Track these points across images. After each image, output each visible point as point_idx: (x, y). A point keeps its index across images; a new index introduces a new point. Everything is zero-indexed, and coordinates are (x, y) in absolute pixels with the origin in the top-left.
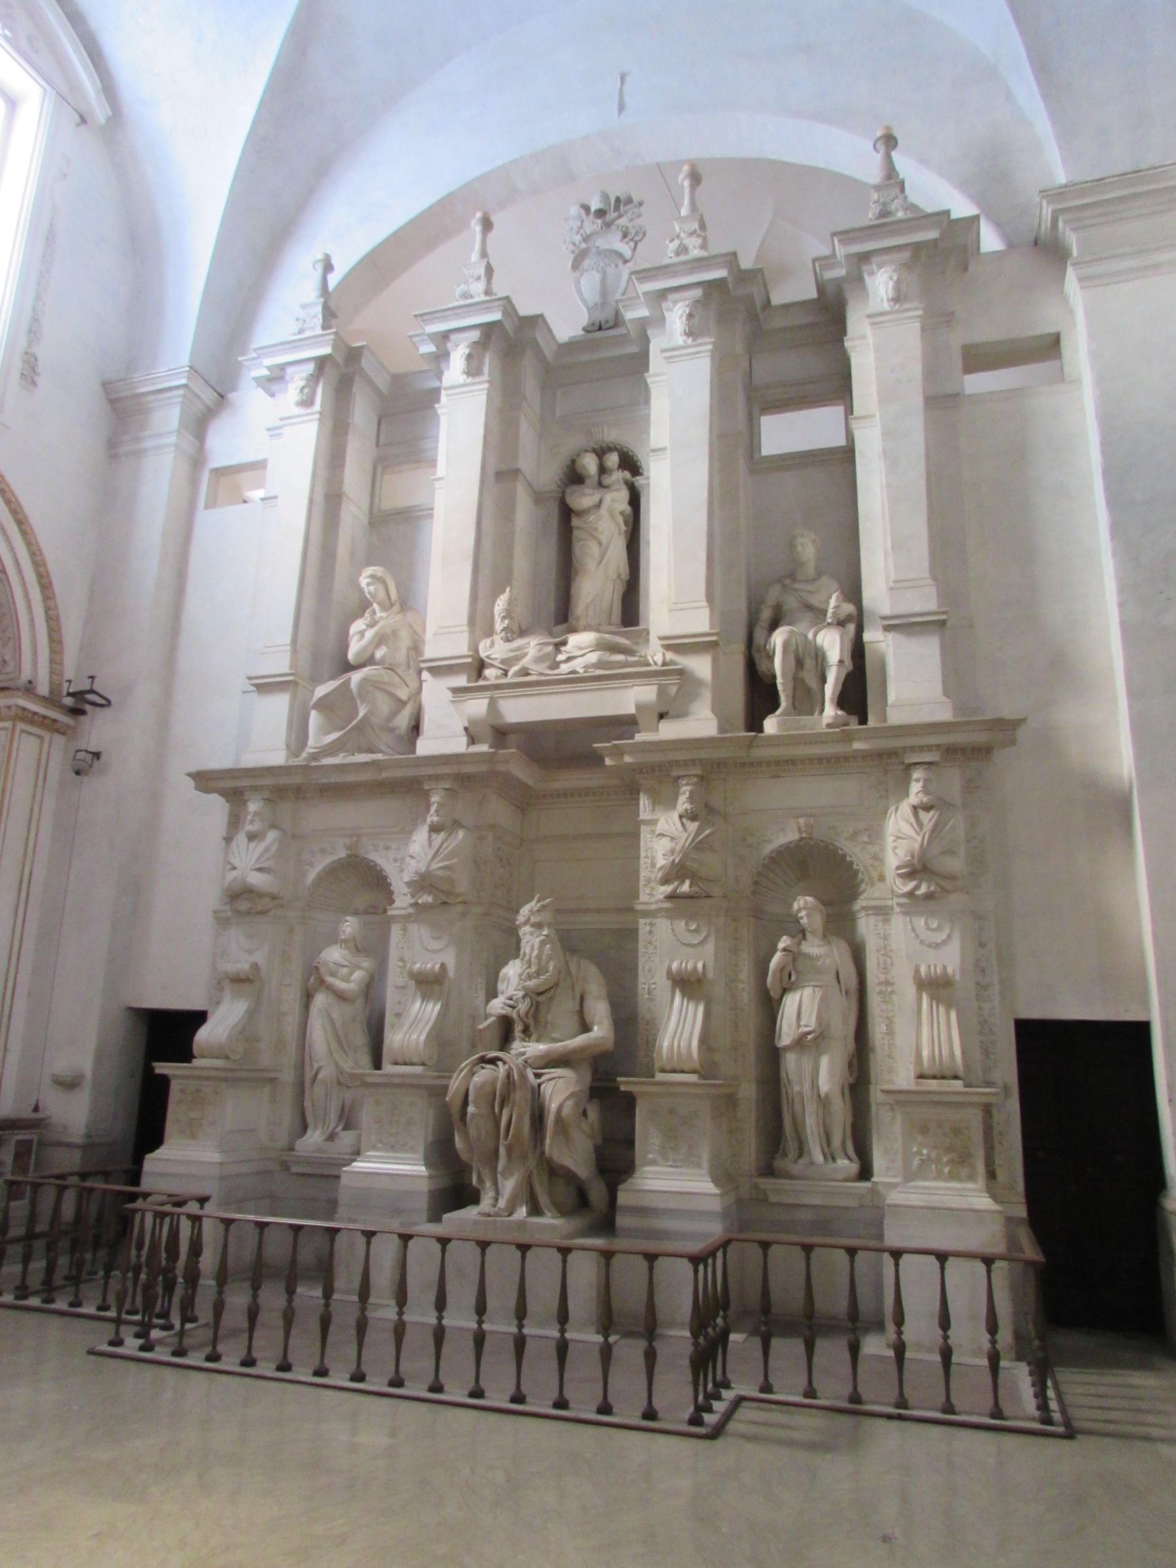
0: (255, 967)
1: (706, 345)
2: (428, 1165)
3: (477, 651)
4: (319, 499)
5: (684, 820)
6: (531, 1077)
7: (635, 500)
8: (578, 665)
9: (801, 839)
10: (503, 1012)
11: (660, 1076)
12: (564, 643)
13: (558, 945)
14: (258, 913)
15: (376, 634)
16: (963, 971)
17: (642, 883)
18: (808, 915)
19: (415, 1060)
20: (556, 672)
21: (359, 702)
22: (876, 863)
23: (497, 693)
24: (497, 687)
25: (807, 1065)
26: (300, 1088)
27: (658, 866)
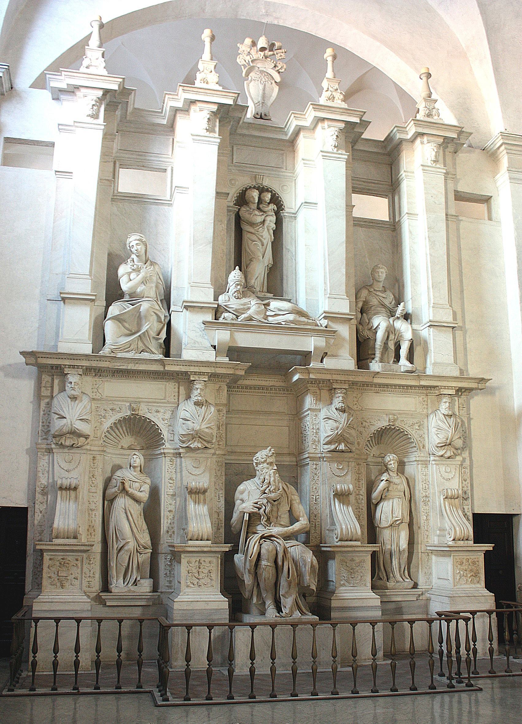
1: (344, 155)
7: (279, 222)
12: (268, 304)
21: (144, 321)
24: (233, 325)
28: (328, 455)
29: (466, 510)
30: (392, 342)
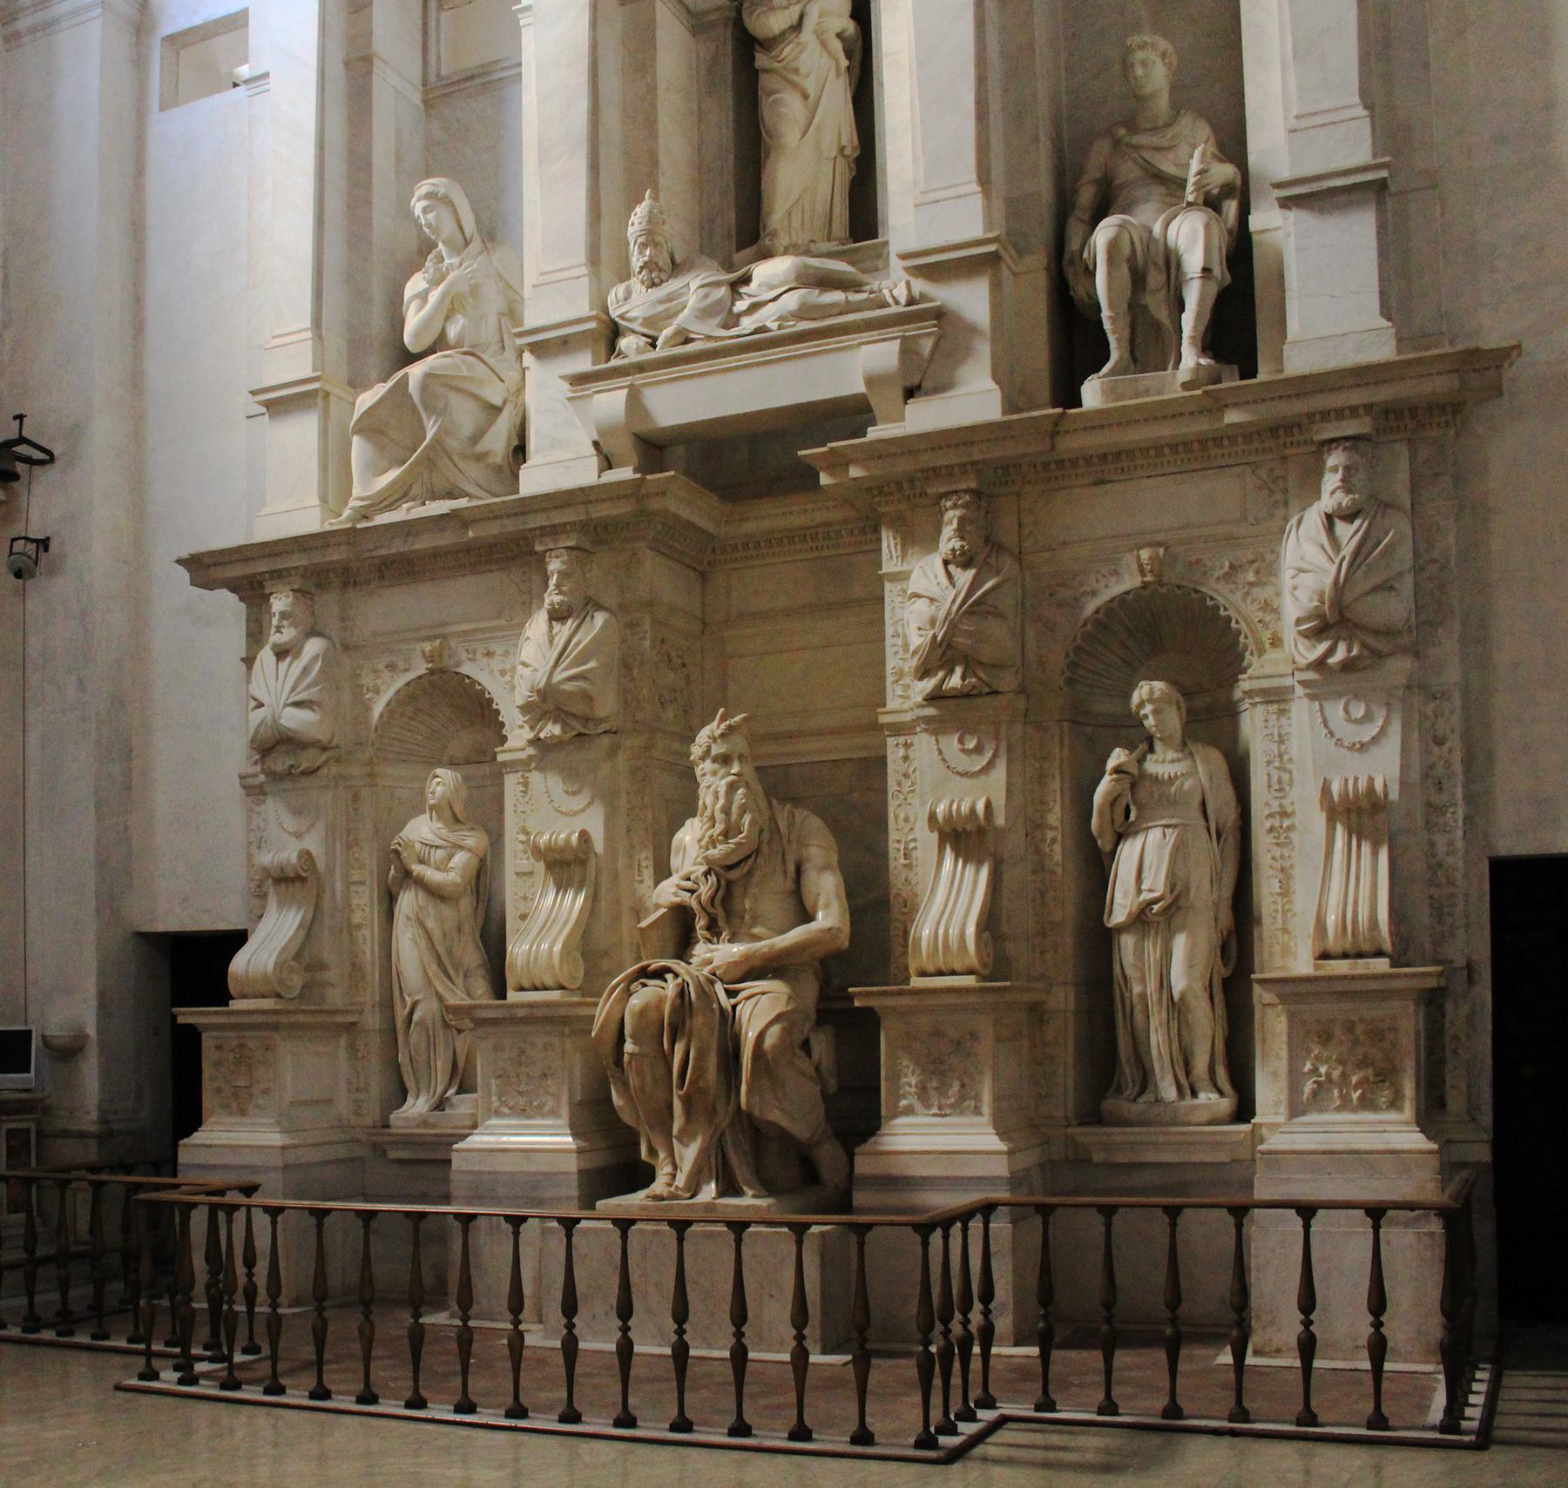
0: (306, 855)
2: (575, 1134)
3: (607, 314)
4: (337, 70)
5: (951, 568)
6: (722, 996)
8: (767, 317)
9: (1145, 585)
10: (677, 900)
11: (917, 982)
13: (758, 787)
14: (303, 773)
15: (444, 296)
16: (1403, 783)
17: (890, 679)
18: (1156, 712)
19: (549, 981)
20: (734, 331)
21: (424, 416)
22: (1268, 618)
23: (639, 379)
24: (640, 368)
25: (1152, 952)
26: (391, 1035)
27: (912, 648)
28: (931, 711)
29: (1441, 848)
30: (1161, 296)
